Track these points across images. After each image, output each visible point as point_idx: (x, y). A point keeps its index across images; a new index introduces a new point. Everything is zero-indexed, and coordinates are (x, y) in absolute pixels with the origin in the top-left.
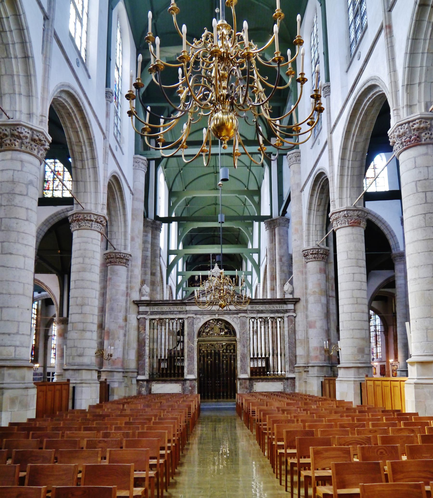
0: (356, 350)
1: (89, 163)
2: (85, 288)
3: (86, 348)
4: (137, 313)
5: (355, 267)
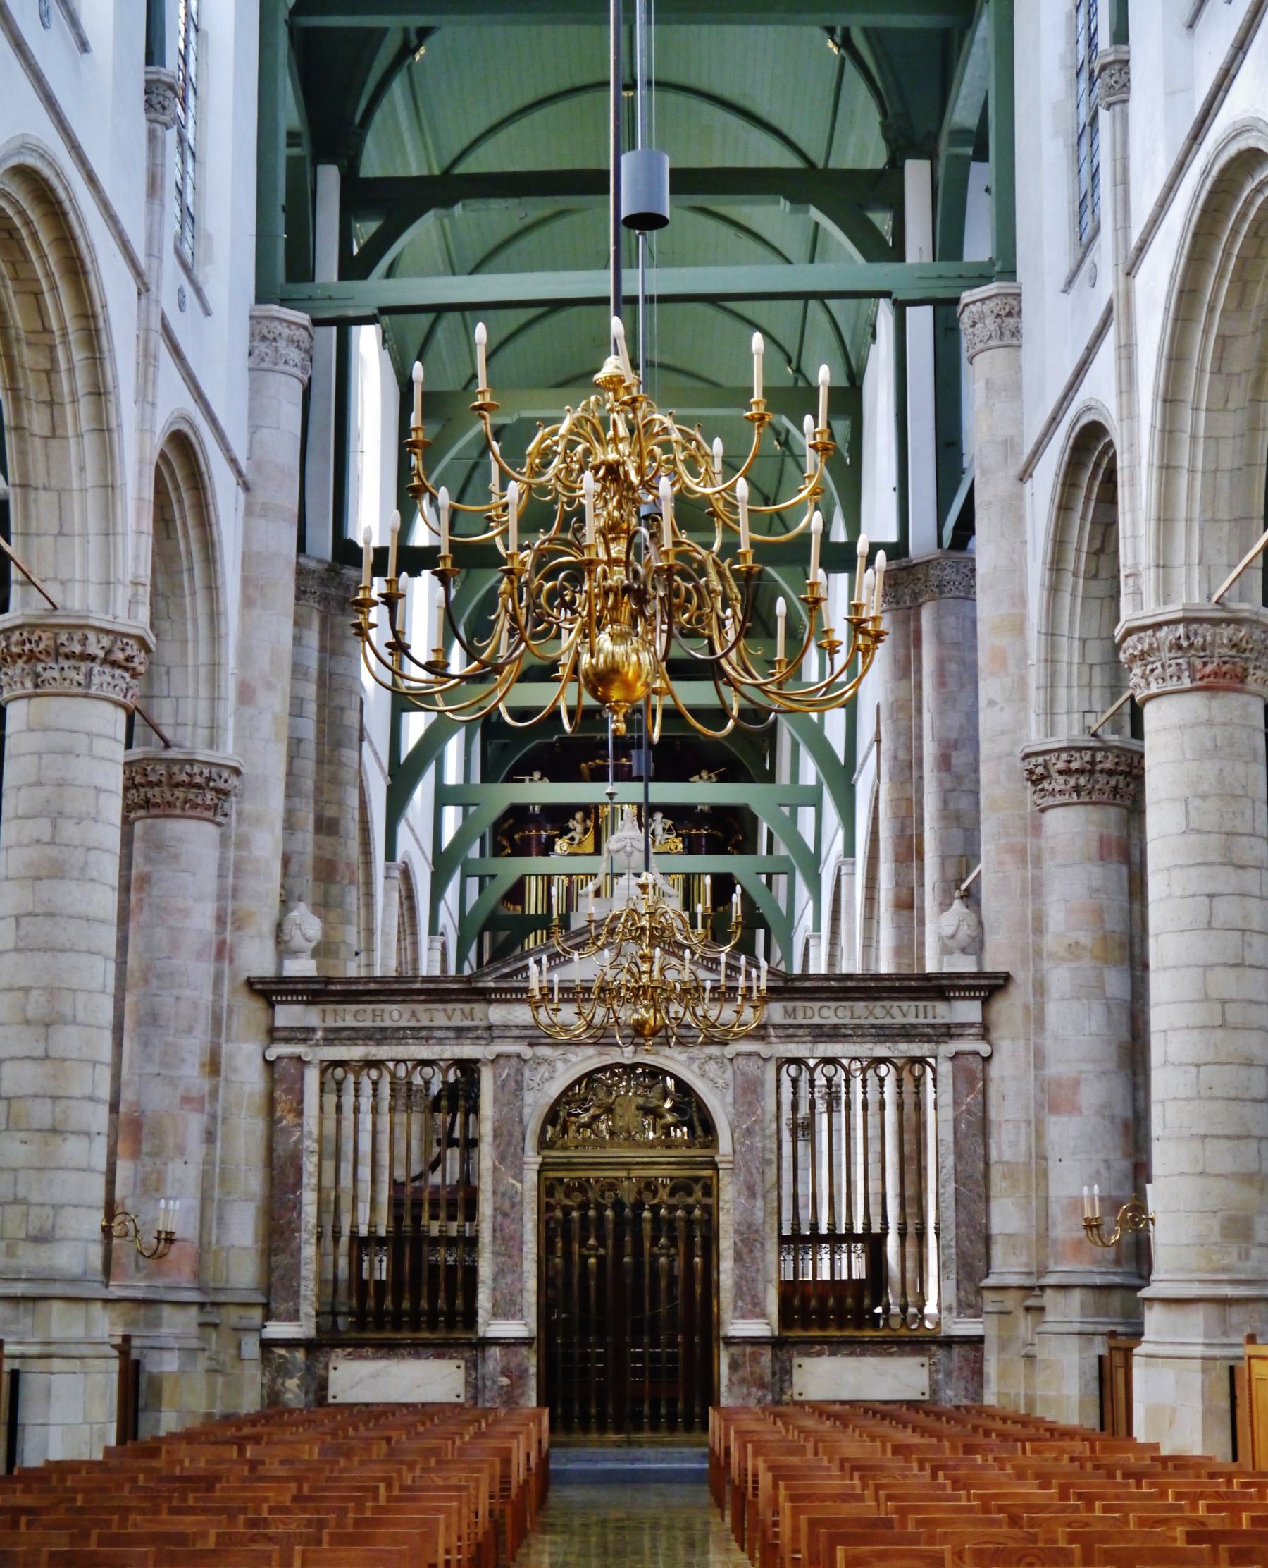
1: (79, 414)
4: (262, 1036)
5: (1218, 869)
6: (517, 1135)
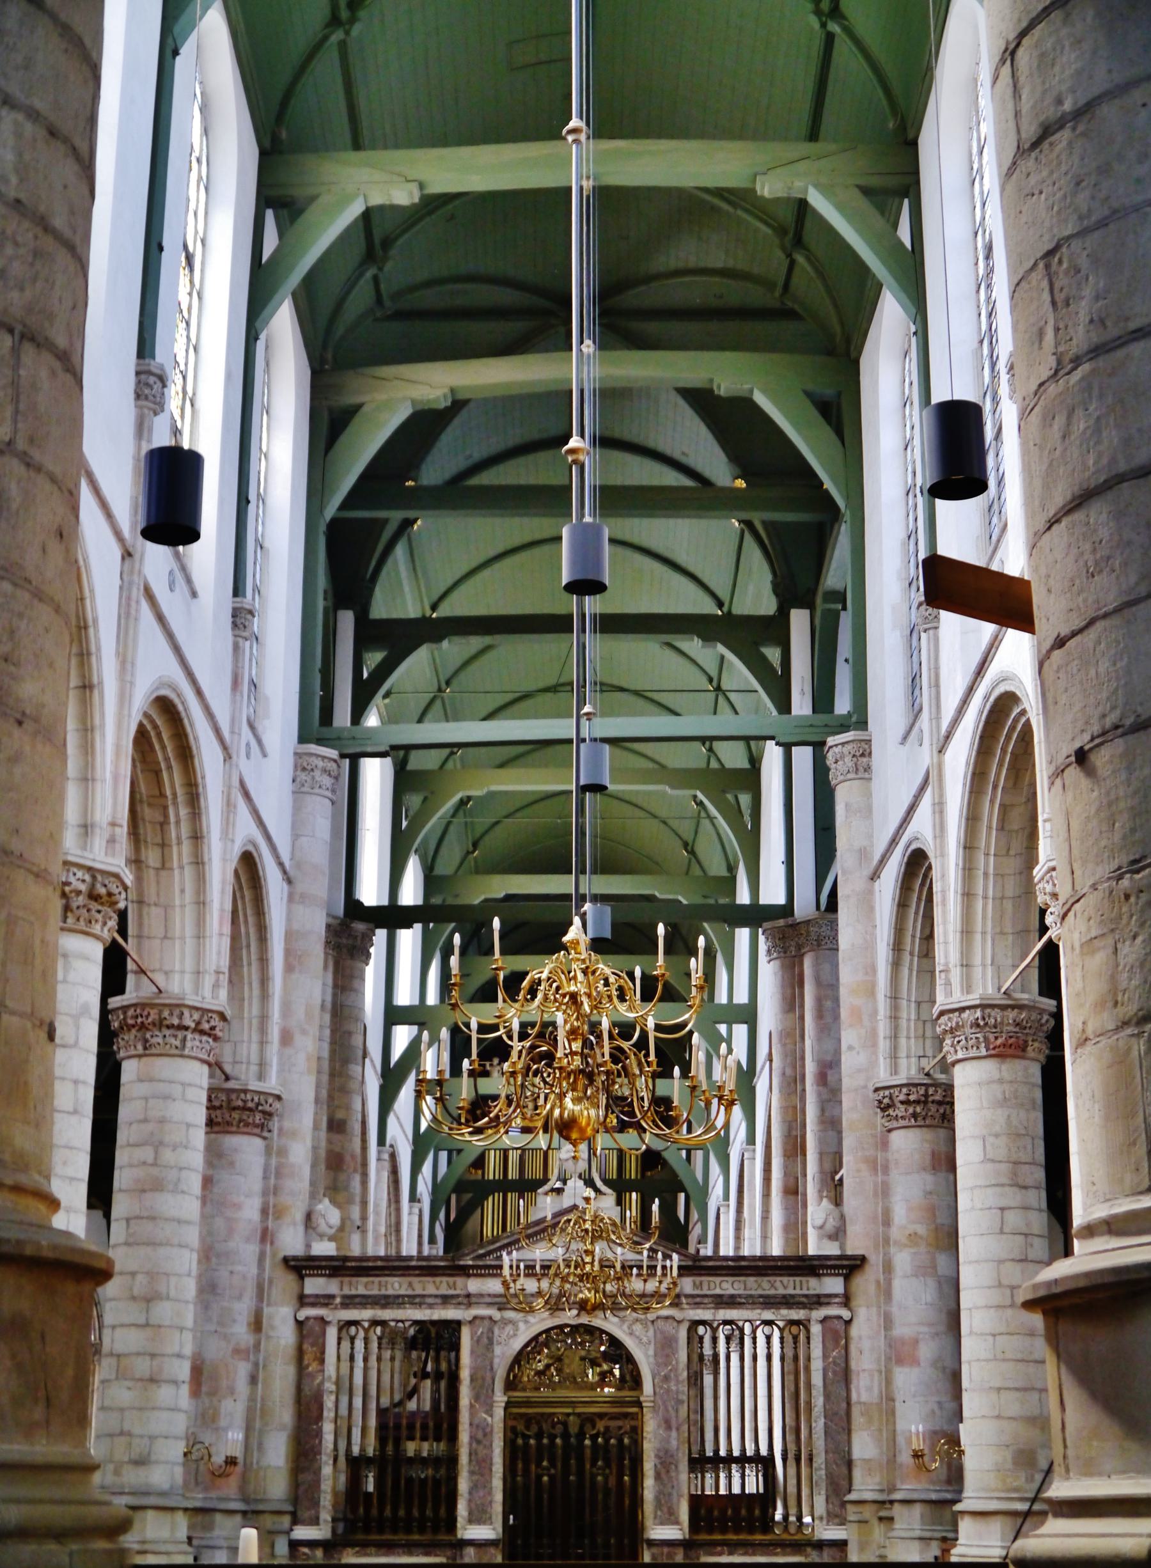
0: (1008, 1455)
1: (181, 853)
2: (160, 1244)
3: (156, 1437)
4: (294, 1301)
5: (1007, 1189)
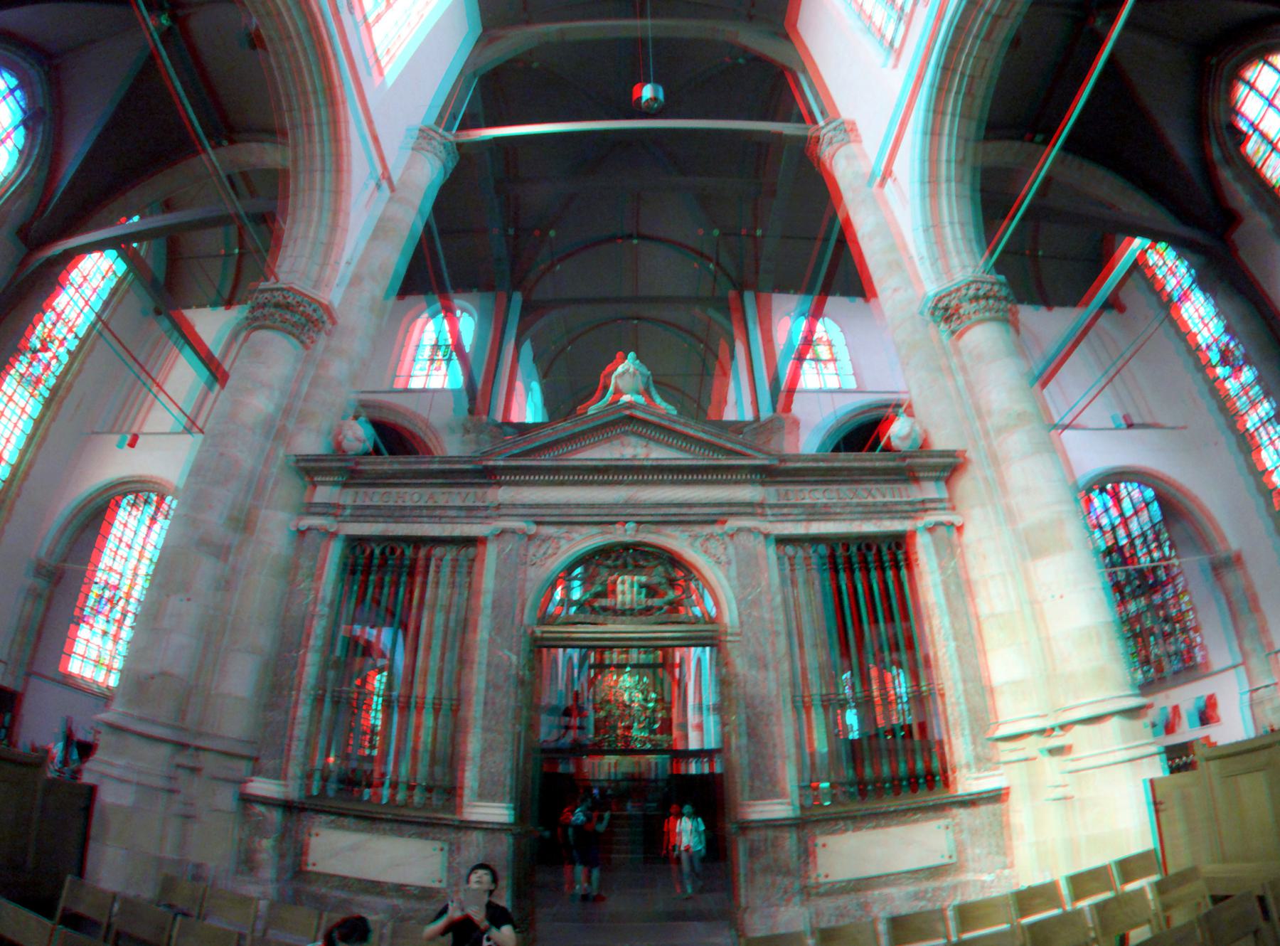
6: (518, 607)
